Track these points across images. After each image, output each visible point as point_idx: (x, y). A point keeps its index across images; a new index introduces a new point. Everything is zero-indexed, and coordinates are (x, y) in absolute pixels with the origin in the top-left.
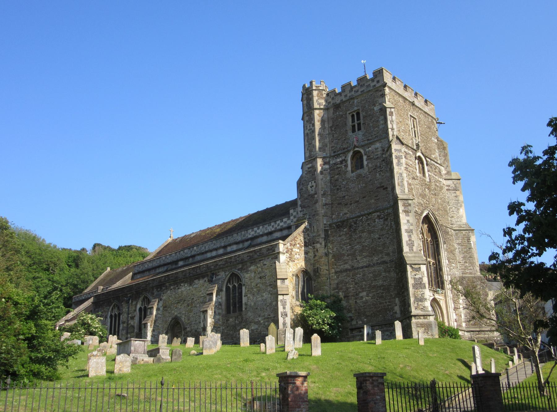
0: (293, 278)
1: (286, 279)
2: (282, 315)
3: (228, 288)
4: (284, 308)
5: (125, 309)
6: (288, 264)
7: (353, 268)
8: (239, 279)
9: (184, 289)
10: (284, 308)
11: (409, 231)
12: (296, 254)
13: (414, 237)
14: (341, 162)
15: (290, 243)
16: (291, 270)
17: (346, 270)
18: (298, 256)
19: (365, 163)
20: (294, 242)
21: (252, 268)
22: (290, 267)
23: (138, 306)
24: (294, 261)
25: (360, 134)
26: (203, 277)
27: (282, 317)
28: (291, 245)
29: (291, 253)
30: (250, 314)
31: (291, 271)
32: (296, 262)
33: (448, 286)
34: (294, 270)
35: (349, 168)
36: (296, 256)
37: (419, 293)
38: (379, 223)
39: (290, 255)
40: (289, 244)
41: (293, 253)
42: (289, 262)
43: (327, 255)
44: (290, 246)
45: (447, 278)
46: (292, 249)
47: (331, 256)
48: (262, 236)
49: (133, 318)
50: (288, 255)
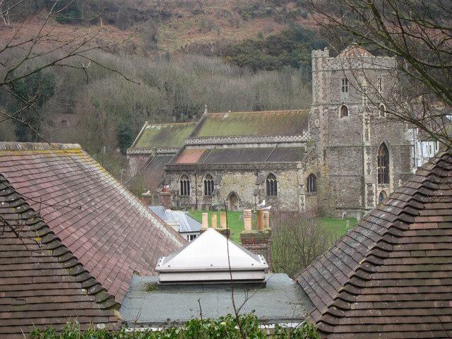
3: (267, 181)
5: (193, 179)
7: (339, 176)
8: (275, 177)
9: (238, 175)
11: (368, 164)
13: (371, 167)
14: (335, 110)
17: (335, 176)
19: (349, 115)
21: (283, 173)
23: (204, 180)
25: (346, 95)
26: (251, 171)
30: (282, 199)
33: (392, 181)
35: (340, 115)
37: (370, 198)
38: (354, 153)
43: (325, 165)
45: (391, 177)
47: (327, 166)
48: (285, 142)
49: (200, 186)
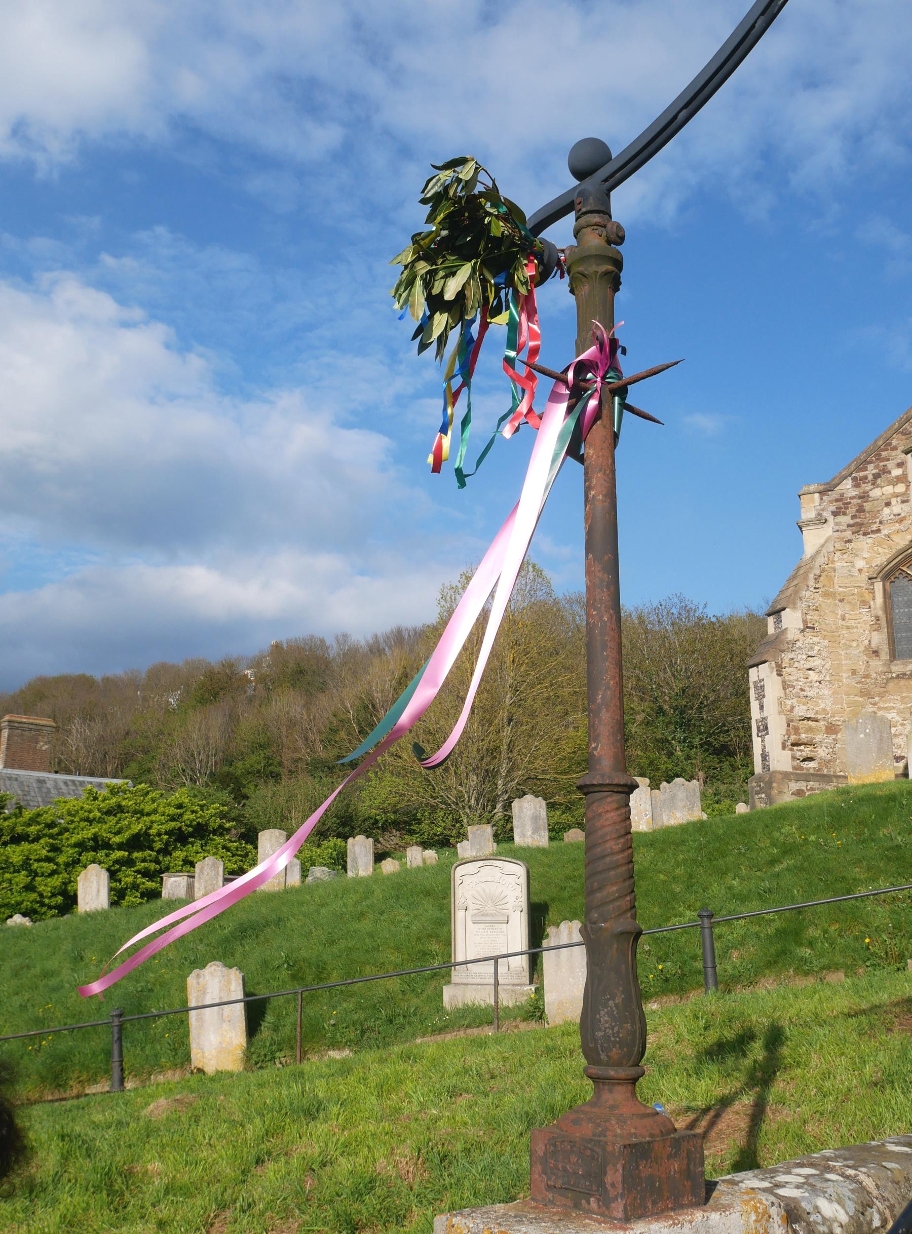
0: (872, 591)
1: (784, 609)
2: (759, 730)
4: (762, 707)
6: (843, 551)
10: (762, 707)
12: (888, 504)
15: (854, 479)
16: (860, 564)
18: (897, 507)
20: (876, 467)
22: (857, 556)
24: (878, 531)
27: (758, 736)
28: (857, 483)
29: (861, 510)
31: (860, 570)
32: (885, 532)
36: (886, 511)
39: (853, 517)
40: (848, 484)
41: (867, 506)
42: (850, 541)
44: (857, 485)
46: (864, 497)
50: (846, 520)
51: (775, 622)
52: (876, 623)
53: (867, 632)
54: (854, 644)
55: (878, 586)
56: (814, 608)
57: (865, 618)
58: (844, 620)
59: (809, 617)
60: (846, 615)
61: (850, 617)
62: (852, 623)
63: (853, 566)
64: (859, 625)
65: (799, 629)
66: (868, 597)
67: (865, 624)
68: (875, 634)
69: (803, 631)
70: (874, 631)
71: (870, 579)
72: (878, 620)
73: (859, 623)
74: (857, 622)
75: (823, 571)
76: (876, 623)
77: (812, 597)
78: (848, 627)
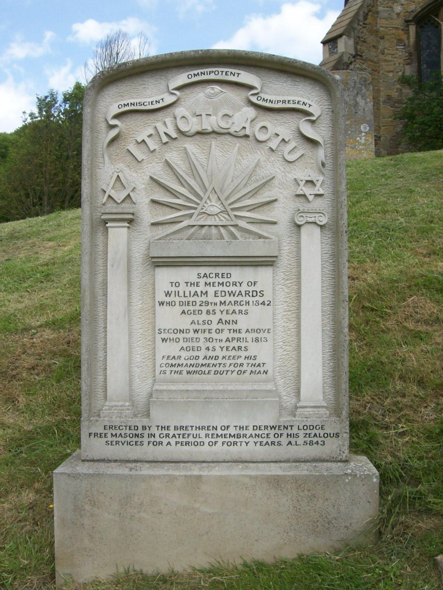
0: (407, 32)
16: (398, 9)
31: (398, 14)
34: (412, 7)
51: (330, 49)
52: (409, 59)
53: (401, 65)
54: (391, 75)
55: (412, 29)
56: (363, 39)
57: (400, 54)
58: (383, 54)
59: (359, 47)
60: (386, 50)
61: (389, 52)
62: (389, 58)
63: (393, 11)
64: (395, 59)
65: (351, 55)
66: (404, 37)
67: (401, 59)
68: (407, 67)
69: (354, 57)
70: (407, 64)
71: (406, 21)
72: (411, 56)
73: (395, 58)
74: (394, 56)
75: (369, 11)
76: (409, 59)
77: (361, 31)
78: (386, 61)
